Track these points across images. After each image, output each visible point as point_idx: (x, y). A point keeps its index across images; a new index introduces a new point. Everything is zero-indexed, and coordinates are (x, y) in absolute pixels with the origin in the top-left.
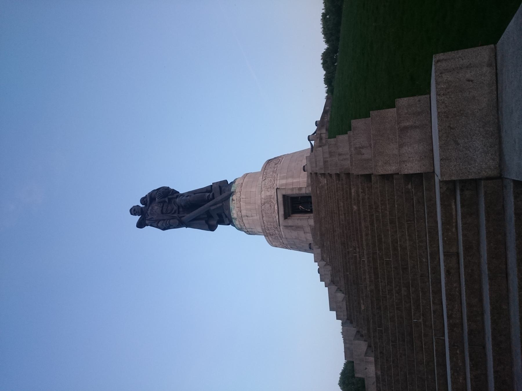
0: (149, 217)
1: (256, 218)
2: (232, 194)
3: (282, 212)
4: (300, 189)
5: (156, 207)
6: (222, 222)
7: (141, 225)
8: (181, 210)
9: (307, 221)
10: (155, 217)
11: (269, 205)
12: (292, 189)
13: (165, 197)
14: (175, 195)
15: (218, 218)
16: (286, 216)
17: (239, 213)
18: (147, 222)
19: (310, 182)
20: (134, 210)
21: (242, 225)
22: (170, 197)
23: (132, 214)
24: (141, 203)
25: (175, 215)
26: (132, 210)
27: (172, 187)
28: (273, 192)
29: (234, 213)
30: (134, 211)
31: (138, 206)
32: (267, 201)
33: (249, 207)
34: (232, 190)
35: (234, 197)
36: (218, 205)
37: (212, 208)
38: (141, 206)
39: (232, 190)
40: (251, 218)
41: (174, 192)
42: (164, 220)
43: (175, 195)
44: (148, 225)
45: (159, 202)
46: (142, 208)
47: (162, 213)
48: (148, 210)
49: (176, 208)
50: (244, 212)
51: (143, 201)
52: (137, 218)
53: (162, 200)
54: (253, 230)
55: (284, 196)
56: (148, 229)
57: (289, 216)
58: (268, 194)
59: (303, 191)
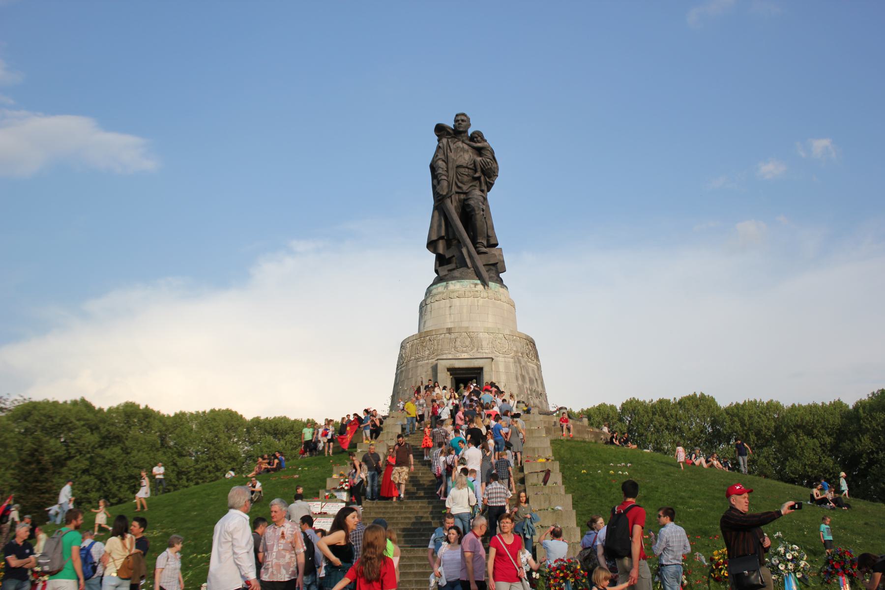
0: (452, 146)
1: (448, 320)
3: (458, 364)
5: (466, 157)
6: (441, 261)
7: (440, 130)
8: (462, 197)
10: (452, 155)
11: (467, 344)
13: (483, 171)
14: (484, 188)
15: (447, 257)
17: (456, 294)
21: (437, 298)
22: (482, 178)
23: (457, 115)
24: (474, 133)
25: (454, 187)
26: (463, 118)
28: (486, 352)
29: (455, 286)
30: (462, 120)
31: (470, 125)
32: (474, 342)
33: (465, 311)
35: (480, 287)
36: (468, 261)
37: (464, 251)
38: (470, 131)
40: (447, 313)
42: (447, 171)
44: (439, 141)
45: (474, 162)
46: (466, 132)
47: (458, 167)
48: (463, 142)
49: (465, 188)
50: (456, 302)
51: (477, 137)
52: (450, 124)
53: (478, 167)
54: (428, 313)
55: (481, 369)
56: (433, 141)
58: (484, 343)
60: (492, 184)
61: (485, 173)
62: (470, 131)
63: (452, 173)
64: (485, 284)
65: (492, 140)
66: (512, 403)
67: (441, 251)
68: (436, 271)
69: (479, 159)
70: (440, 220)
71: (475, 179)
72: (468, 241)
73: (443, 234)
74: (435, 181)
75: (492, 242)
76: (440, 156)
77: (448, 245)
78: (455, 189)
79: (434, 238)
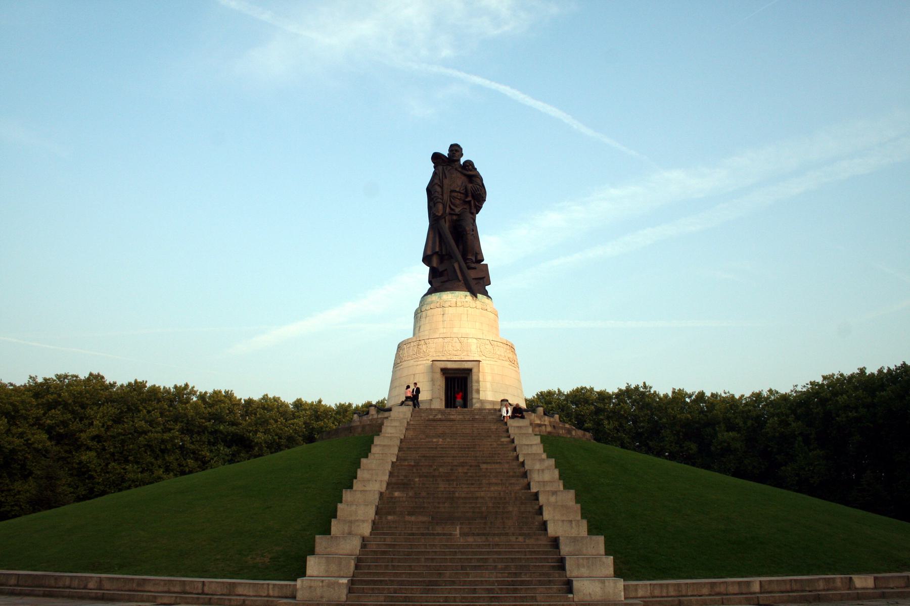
2: (474, 294)
3: (450, 365)
4: (478, 391)
7: (436, 157)
9: (431, 394)
12: (478, 382)
13: (473, 196)
14: (474, 211)
15: (441, 269)
16: (444, 371)
18: (440, 168)
19: (488, 406)
20: (457, 151)
23: (452, 146)
24: (466, 162)
25: (448, 210)
27: (485, 205)
29: (448, 297)
30: (456, 150)
34: (479, 295)
37: (456, 266)
38: (462, 160)
39: (479, 295)
41: (478, 209)
43: (474, 211)
45: (466, 188)
46: (459, 160)
51: (469, 165)
52: (445, 152)
54: (423, 320)
56: (430, 168)
57: (444, 374)
58: (474, 347)
59: (475, 395)
60: (480, 208)
62: (462, 160)
63: (446, 197)
67: (435, 265)
68: (430, 282)
69: (470, 186)
70: (434, 237)
71: (466, 202)
72: (459, 257)
73: (437, 249)
74: (432, 203)
75: (479, 258)
76: (436, 181)
77: (442, 259)
78: (448, 210)
79: (429, 253)
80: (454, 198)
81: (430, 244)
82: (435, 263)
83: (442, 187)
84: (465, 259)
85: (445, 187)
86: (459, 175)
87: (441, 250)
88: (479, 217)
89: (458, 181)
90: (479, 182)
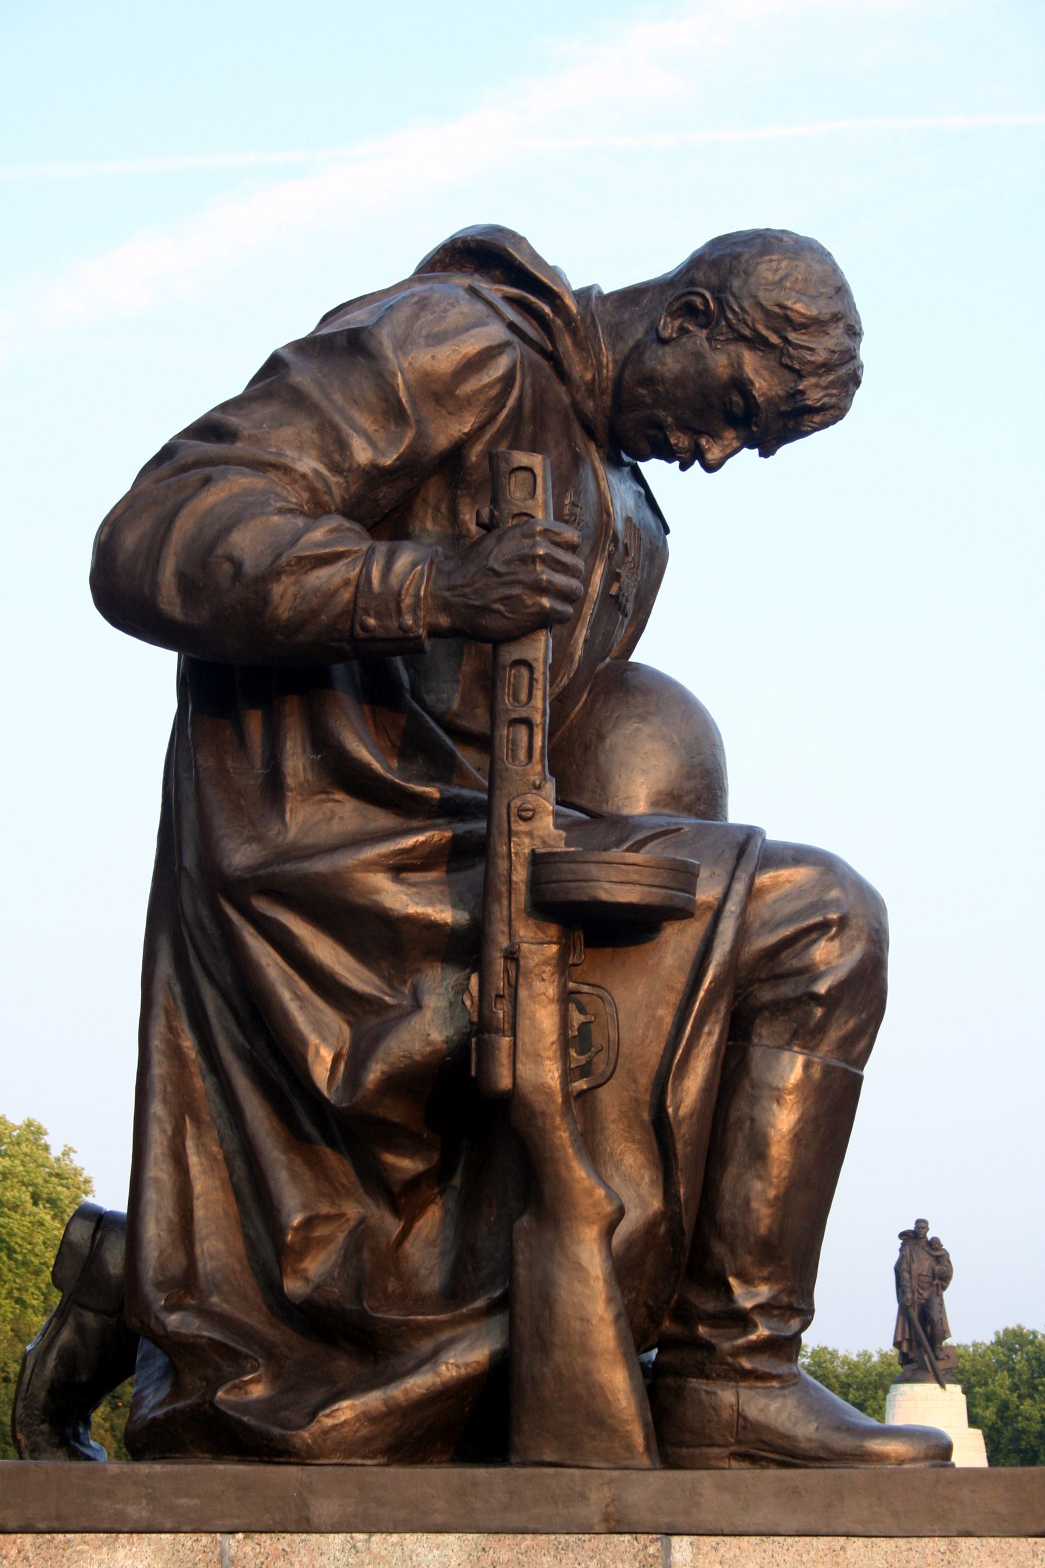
7: (903, 1235)
25: (916, 1294)
30: (922, 1225)
36: (929, 1367)
37: (926, 1358)
41: (944, 1288)
45: (933, 1272)
46: (925, 1236)
47: (920, 1275)
51: (934, 1245)
52: (911, 1227)
61: (942, 1276)
62: (929, 1236)
63: (915, 1283)
64: (943, 1386)
65: (946, 1245)
66: (967, 1364)
67: (905, 1349)
69: (937, 1268)
72: (929, 1348)
73: (907, 1336)
77: (910, 1348)
78: (916, 1294)
79: (899, 1339)
80: (922, 1281)
81: (900, 1330)
82: (905, 1349)
83: (910, 1273)
84: (934, 1351)
85: (913, 1273)
86: (926, 1256)
87: (910, 1335)
88: (946, 1294)
89: (924, 1264)
90: (946, 1263)
